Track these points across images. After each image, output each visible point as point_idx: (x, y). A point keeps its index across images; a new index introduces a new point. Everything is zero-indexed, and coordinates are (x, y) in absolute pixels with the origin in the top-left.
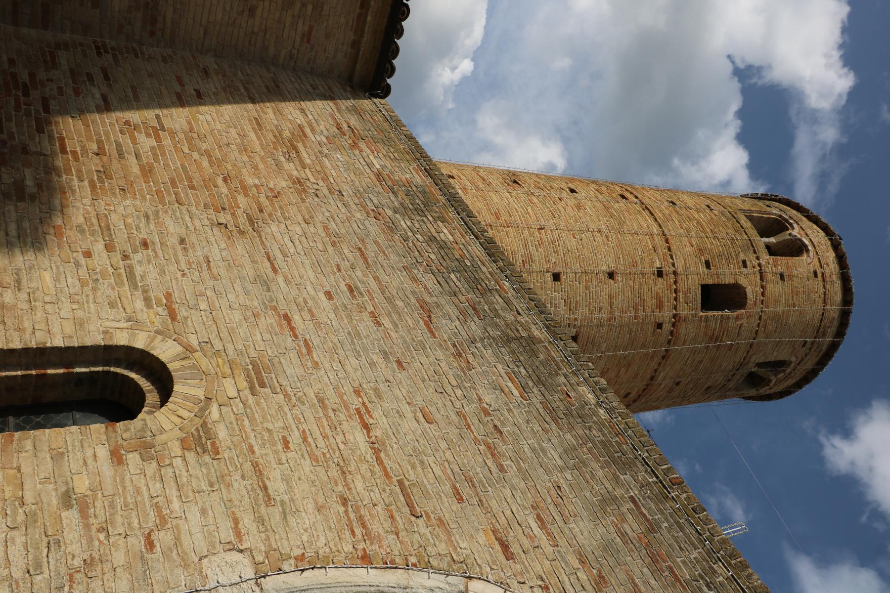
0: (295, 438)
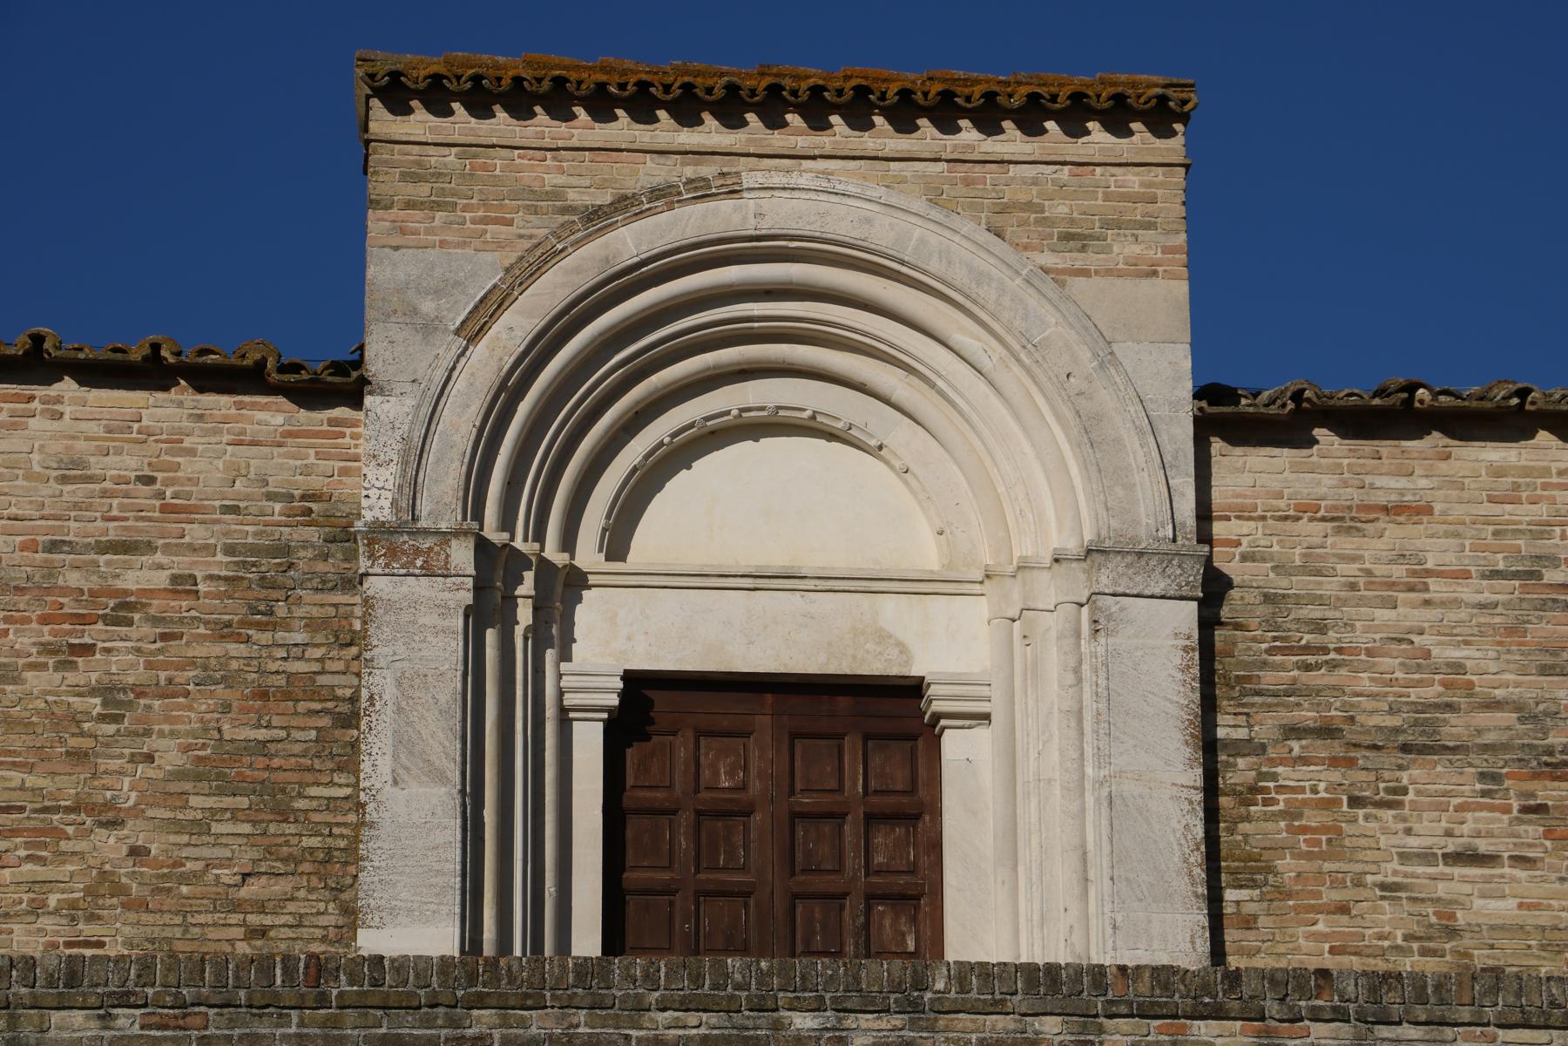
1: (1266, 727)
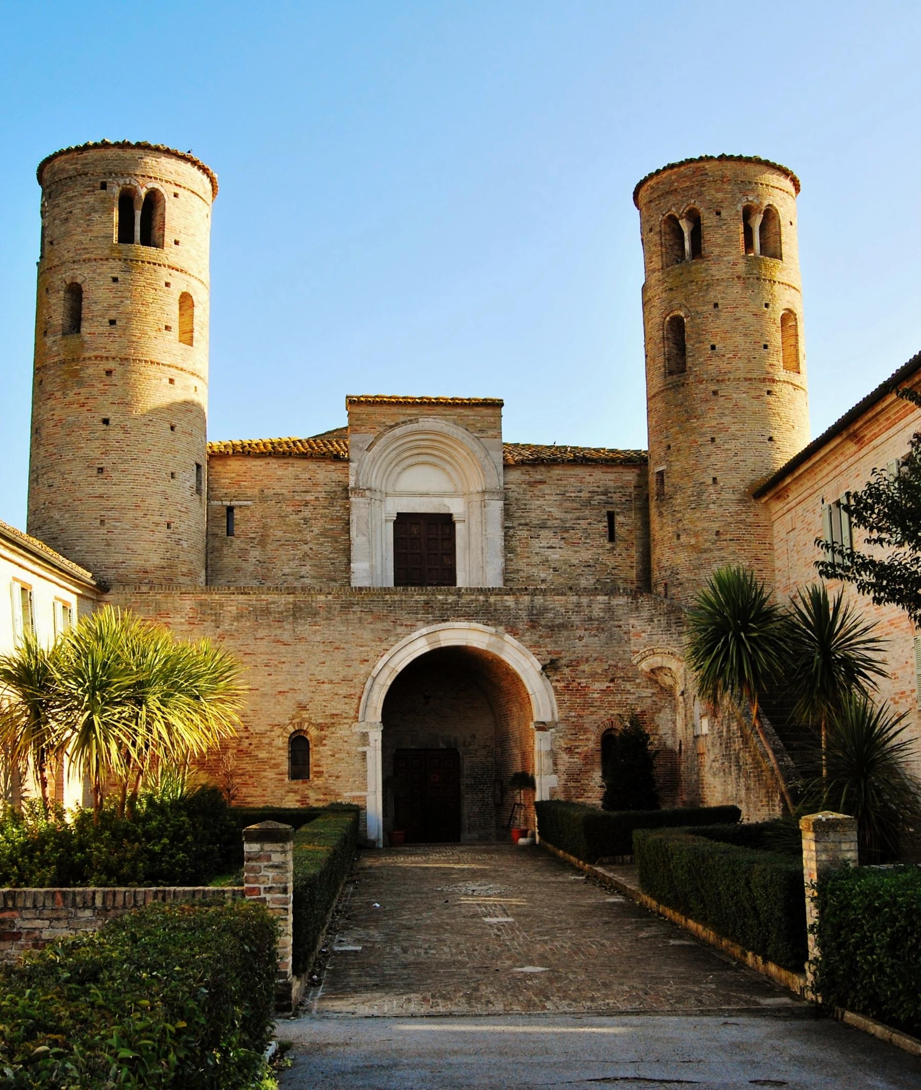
0: (324, 704)
1: (515, 524)
